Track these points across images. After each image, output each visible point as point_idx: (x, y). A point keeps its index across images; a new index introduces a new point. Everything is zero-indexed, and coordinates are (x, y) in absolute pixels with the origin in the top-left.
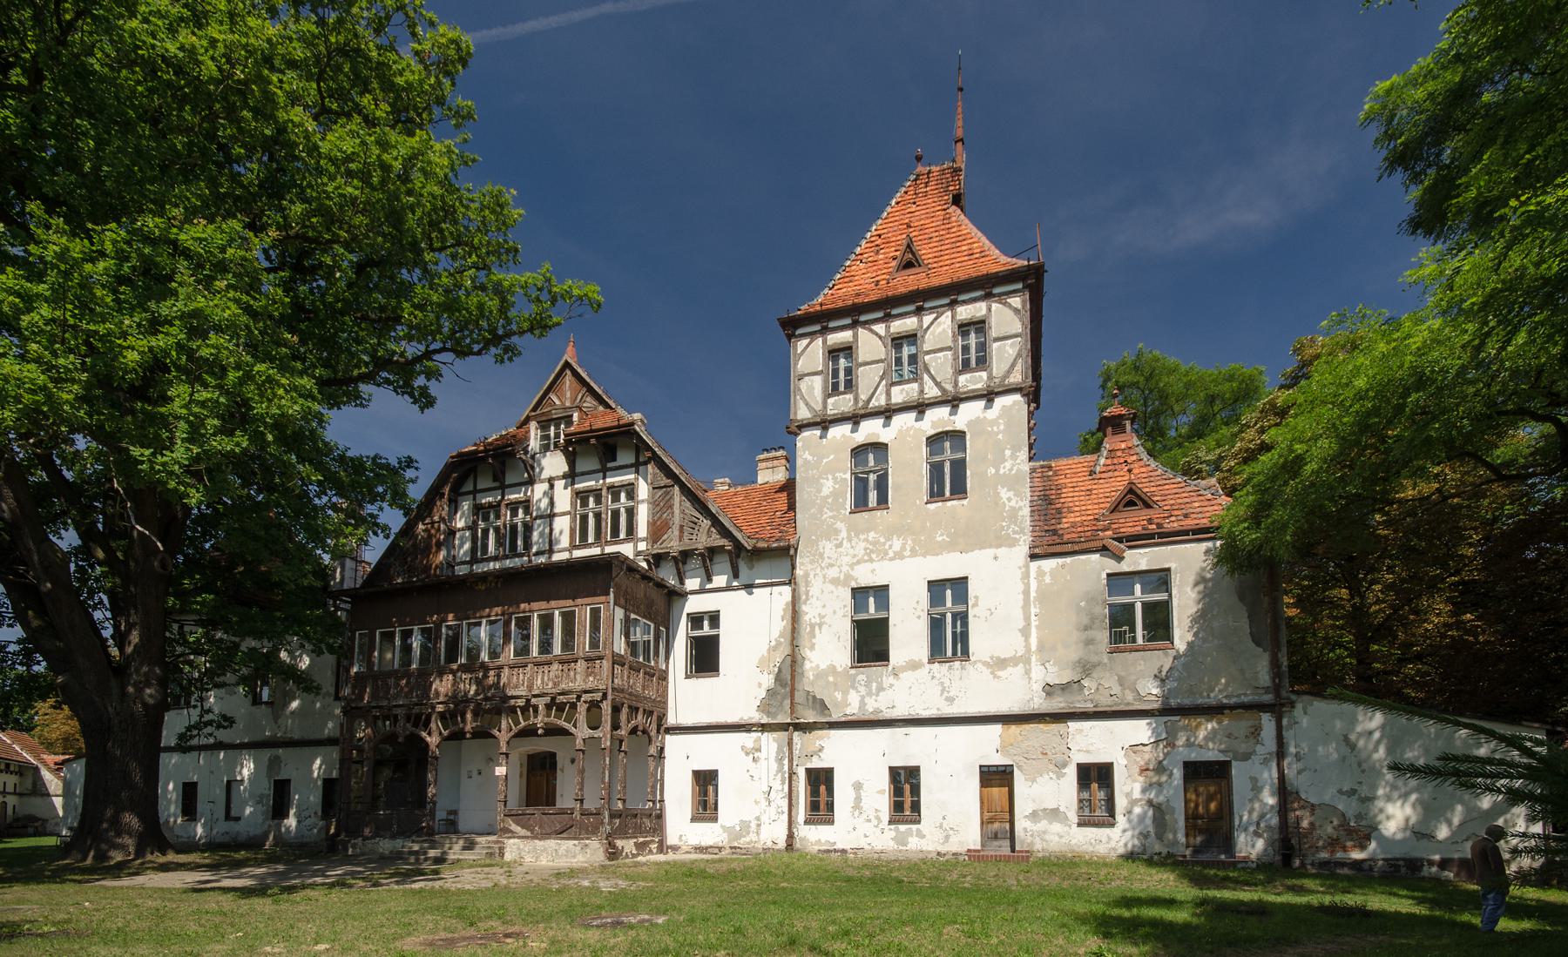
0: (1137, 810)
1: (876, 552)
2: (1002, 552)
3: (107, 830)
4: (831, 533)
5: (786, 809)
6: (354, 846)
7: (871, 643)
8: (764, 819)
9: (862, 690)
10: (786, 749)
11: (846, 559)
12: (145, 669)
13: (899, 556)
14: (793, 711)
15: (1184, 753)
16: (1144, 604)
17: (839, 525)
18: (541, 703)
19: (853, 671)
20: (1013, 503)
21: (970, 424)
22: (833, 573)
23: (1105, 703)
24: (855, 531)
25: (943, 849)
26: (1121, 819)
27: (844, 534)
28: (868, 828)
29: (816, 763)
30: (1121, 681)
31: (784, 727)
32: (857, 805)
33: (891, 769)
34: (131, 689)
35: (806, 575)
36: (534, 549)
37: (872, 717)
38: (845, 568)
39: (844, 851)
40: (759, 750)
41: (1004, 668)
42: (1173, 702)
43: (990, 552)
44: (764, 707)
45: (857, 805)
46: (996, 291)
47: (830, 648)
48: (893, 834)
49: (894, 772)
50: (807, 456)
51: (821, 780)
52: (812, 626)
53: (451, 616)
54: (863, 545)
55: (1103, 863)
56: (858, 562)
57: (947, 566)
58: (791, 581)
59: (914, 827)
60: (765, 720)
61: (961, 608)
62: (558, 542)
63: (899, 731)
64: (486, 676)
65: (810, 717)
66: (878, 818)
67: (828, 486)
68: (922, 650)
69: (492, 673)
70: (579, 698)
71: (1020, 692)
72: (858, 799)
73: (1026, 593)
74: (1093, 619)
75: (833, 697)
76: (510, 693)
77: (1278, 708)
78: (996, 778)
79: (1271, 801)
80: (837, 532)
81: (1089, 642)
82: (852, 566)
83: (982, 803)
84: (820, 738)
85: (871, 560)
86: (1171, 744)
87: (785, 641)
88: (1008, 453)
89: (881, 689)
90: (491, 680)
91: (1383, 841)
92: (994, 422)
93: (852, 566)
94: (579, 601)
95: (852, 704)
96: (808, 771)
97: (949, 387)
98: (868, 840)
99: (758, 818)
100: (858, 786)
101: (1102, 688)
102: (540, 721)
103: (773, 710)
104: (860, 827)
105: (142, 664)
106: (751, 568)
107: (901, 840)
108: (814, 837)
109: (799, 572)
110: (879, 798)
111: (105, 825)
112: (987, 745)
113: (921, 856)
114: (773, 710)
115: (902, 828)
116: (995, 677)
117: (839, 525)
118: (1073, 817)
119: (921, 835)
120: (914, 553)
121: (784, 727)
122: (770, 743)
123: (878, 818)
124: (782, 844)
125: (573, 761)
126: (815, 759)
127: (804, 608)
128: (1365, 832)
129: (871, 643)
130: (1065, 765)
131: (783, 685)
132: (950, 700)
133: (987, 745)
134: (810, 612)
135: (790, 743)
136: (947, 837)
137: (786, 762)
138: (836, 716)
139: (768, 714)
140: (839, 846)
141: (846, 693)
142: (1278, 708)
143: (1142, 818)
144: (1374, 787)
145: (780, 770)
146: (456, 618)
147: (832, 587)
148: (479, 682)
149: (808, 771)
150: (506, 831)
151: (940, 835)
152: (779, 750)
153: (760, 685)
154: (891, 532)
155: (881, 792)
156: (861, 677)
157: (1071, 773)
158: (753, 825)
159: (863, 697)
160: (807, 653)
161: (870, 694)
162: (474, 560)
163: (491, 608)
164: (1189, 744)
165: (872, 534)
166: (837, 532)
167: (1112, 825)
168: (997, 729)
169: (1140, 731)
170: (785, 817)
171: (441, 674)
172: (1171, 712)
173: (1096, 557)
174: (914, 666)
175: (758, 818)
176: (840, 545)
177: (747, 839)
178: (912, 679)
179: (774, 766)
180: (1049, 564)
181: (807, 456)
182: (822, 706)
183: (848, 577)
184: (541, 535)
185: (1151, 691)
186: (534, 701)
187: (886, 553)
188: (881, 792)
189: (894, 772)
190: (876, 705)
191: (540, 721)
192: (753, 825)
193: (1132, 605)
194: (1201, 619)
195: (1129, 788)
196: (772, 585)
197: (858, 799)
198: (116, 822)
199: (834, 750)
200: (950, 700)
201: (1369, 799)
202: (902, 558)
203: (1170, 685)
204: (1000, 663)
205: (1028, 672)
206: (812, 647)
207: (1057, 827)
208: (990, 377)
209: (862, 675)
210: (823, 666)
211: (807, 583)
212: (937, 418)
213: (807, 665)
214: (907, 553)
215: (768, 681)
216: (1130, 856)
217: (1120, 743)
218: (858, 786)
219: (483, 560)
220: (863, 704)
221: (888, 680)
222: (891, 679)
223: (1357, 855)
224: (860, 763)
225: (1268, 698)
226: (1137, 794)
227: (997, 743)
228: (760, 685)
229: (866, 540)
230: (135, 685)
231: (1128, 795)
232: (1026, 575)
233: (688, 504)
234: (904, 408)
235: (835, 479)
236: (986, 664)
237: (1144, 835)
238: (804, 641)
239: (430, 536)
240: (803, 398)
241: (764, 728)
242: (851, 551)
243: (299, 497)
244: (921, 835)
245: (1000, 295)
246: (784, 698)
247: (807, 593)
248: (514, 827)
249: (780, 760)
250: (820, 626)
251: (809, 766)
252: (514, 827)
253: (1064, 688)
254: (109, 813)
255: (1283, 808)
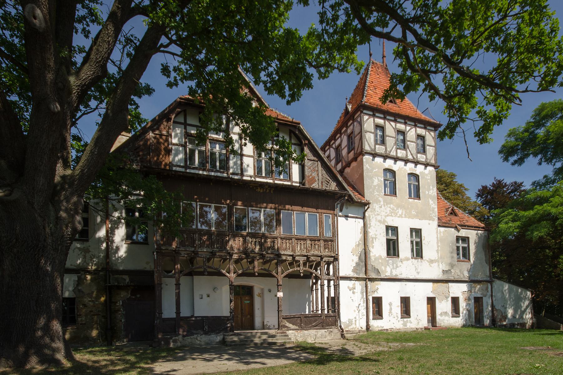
0: (465, 312)
1: (393, 213)
2: (431, 222)
3: (42, 337)
4: (378, 201)
5: (365, 314)
6: (175, 341)
7: (392, 248)
8: (357, 318)
9: (391, 266)
10: (365, 288)
11: (383, 213)
12: (75, 199)
13: (401, 216)
14: (367, 275)
15: (474, 295)
16: (462, 247)
17: (380, 199)
18: (302, 260)
19: (387, 259)
20: (433, 206)
21: (420, 173)
22: (379, 218)
23: (457, 278)
24: (387, 203)
25: (418, 327)
26: (461, 314)
27: (382, 203)
28: (394, 320)
29: (376, 295)
30: (460, 271)
31: (365, 279)
32: (390, 312)
33: (401, 298)
34: (63, 214)
35: (369, 217)
36: (231, 171)
37: (395, 277)
38: (383, 217)
39: (387, 330)
40: (355, 289)
41: (432, 263)
42: (473, 279)
43: (427, 221)
44: (355, 270)
45: (390, 312)
46: (428, 128)
47: (378, 249)
48: (402, 322)
49: (402, 298)
50: (367, 166)
51: (378, 302)
52: (373, 238)
53: (240, 203)
54: (389, 209)
55: (457, 329)
56: (388, 216)
57: (417, 225)
58: (364, 218)
59: (409, 319)
60: (356, 276)
61: (419, 240)
62: (247, 171)
63: (403, 283)
64: (265, 242)
65: (373, 276)
66: (397, 316)
67: (376, 182)
68: (409, 254)
69: (269, 240)
70: (322, 259)
71: (436, 274)
72: (391, 309)
73: (437, 238)
74: (453, 250)
75: (382, 268)
76: (282, 252)
77: (491, 282)
78: (431, 301)
79: (490, 309)
80: (380, 201)
81: (452, 257)
82: (386, 216)
83: (339, 311)
84: (377, 285)
85: (392, 216)
86: (471, 292)
87: (362, 243)
88: (431, 187)
89: (397, 267)
90: (269, 244)
91: (509, 319)
92: (427, 175)
93: (386, 216)
94: (320, 211)
95: (388, 272)
96: (373, 298)
97: (415, 157)
98: (394, 325)
99: (355, 318)
100: (390, 304)
101: (456, 273)
102: (302, 269)
103: (358, 272)
104: (391, 321)
105: (72, 194)
106: (347, 208)
107: (405, 324)
108: (376, 325)
109: (367, 214)
110: (397, 309)
111: (39, 333)
112: (428, 290)
113: (411, 330)
114: (358, 272)
115: (405, 320)
116: (431, 266)
117: (380, 199)
118: (450, 315)
119: (411, 323)
120: (405, 217)
121: (365, 279)
122: (359, 285)
123: (397, 316)
124: (364, 328)
125: (270, 291)
126: (376, 293)
127: (369, 230)
128: (505, 317)
129: (392, 248)
130: (448, 297)
131: (362, 262)
132: (418, 273)
133: (428, 290)
134: (371, 232)
135: (366, 287)
136: (418, 323)
137: (365, 294)
138: (383, 276)
139: (357, 273)
140: (385, 328)
141: (386, 267)
142: (491, 282)
143: (466, 314)
144: (507, 305)
145: (363, 297)
146: (243, 205)
147: (379, 224)
148: (261, 245)
149: (373, 298)
150: (285, 326)
151: (416, 322)
152: (362, 289)
153: (353, 260)
154: (398, 206)
155: (398, 306)
156: (390, 261)
157: (450, 299)
158: (354, 321)
159: (391, 270)
160: (371, 249)
161: (393, 268)
162: (186, 167)
163: (267, 203)
164: (475, 292)
165: (392, 206)
166: (380, 201)
167: (459, 317)
168: (431, 284)
169: (464, 287)
170: (365, 317)
171: (234, 236)
172: (472, 281)
173: (453, 229)
174: (407, 259)
175: (355, 318)
176: (381, 207)
177: (352, 327)
178: (406, 266)
179: (360, 296)
180: (442, 229)
181: (367, 166)
182: (378, 272)
183: (384, 221)
184: (235, 163)
185: (466, 275)
186: (297, 258)
187: (397, 214)
188: (398, 306)
189: (402, 298)
190: (396, 273)
191: (302, 269)
192: (354, 321)
193: (462, 247)
194: (476, 254)
195: (463, 305)
196: (357, 218)
197: (391, 309)
198: (47, 329)
199: (385, 291)
200: (418, 273)
201: (506, 308)
202: (402, 217)
203: (471, 273)
204: (431, 261)
205: (439, 265)
206: (373, 247)
207: (447, 318)
208: (427, 158)
209: (391, 260)
210: (377, 256)
211: (370, 220)
212: (389, 163)
213: (371, 254)
214: (403, 216)
215: (356, 259)
216: (464, 326)
217: (459, 290)
218: (390, 304)
219: (190, 168)
220: (391, 272)
221: (399, 264)
222: (400, 263)
223: (505, 323)
224: (390, 294)
225: (488, 279)
226: (464, 307)
227: (431, 290)
228: (353, 260)
229: (390, 207)
230: (67, 210)
231: (463, 307)
232: (437, 232)
233: (324, 172)
234: (401, 160)
235: (378, 179)
236: (427, 261)
237: (466, 320)
238: (369, 244)
239: (159, 143)
240: (367, 141)
241: (358, 279)
242: (385, 211)
243: (225, 107)
244: (411, 323)
245: (429, 130)
246: (362, 267)
247: (370, 224)
248: (288, 324)
249: (362, 293)
250: (375, 238)
251: (374, 296)
252: (288, 324)
253: (447, 271)
254: (42, 322)
255: (492, 311)
